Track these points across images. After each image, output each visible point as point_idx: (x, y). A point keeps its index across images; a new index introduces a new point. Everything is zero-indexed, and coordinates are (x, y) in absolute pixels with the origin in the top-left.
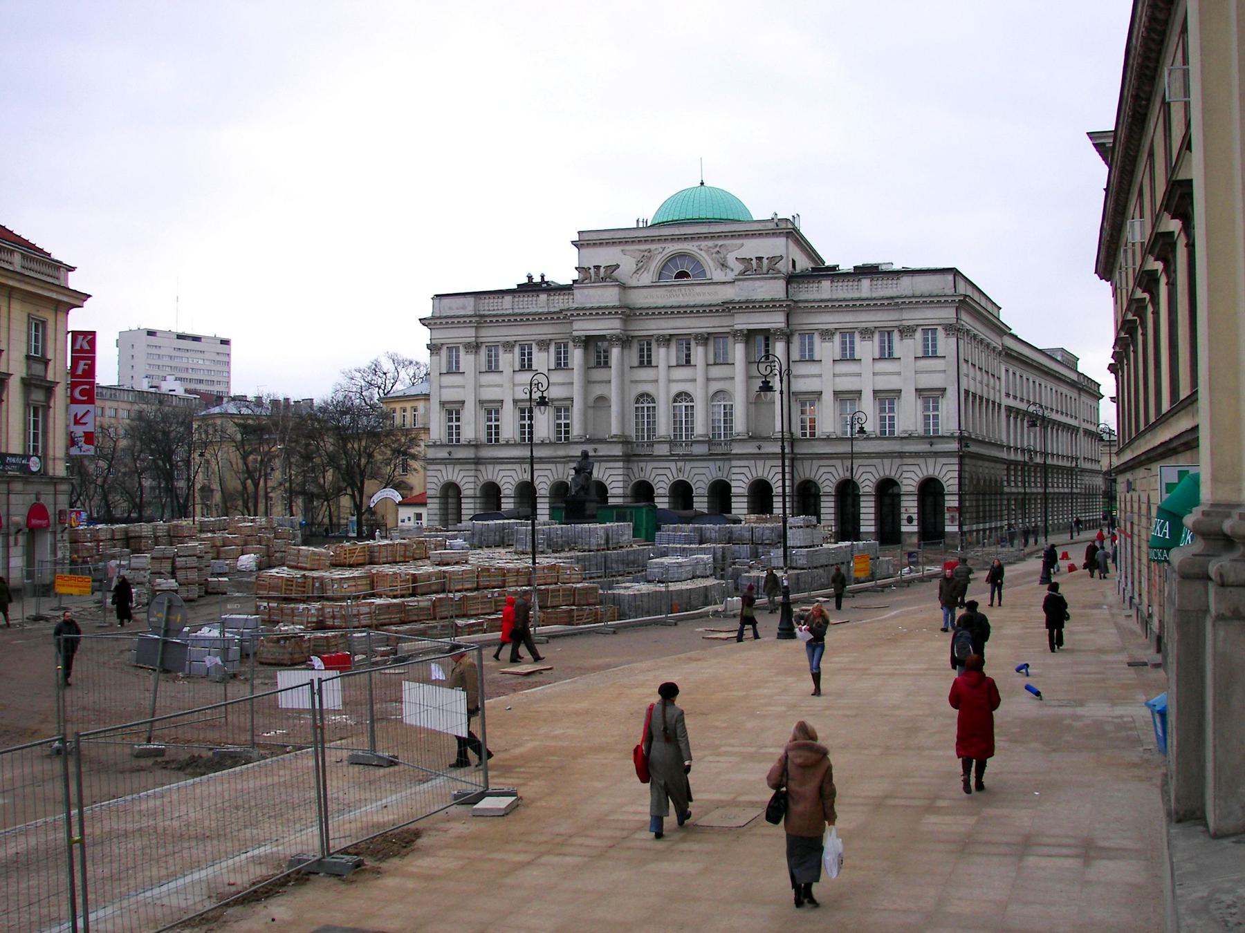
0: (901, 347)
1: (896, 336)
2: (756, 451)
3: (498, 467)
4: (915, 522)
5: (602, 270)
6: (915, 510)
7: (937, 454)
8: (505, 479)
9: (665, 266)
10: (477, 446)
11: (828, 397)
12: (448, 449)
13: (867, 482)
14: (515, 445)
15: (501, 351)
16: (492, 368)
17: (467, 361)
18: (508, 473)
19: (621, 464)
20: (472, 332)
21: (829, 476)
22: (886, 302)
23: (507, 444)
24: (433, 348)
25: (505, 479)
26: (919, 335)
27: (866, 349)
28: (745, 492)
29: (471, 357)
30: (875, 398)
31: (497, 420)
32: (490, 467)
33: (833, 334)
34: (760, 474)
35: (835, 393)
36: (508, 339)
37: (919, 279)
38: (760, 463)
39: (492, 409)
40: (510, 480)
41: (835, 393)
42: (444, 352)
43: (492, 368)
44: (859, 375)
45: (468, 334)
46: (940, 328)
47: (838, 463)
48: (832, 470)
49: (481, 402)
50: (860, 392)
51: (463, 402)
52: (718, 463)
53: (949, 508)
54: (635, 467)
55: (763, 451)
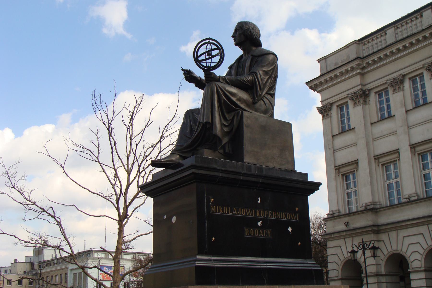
3: (403, 233)
8: (412, 248)
10: (373, 209)
12: (346, 219)
14: (419, 200)
15: (390, 91)
16: (386, 115)
17: (356, 113)
18: (414, 239)
20: (357, 80)
23: (410, 202)
24: (324, 111)
25: (412, 248)
29: (359, 109)
31: (396, 177)
32: (393, 234)
36: (395, 75)
39: (387, 161)
40: (417, 248)
42: (334, 112)
43: (386, 115)
45: (353, 83)
49: (377, 158)
51: (356, 162)
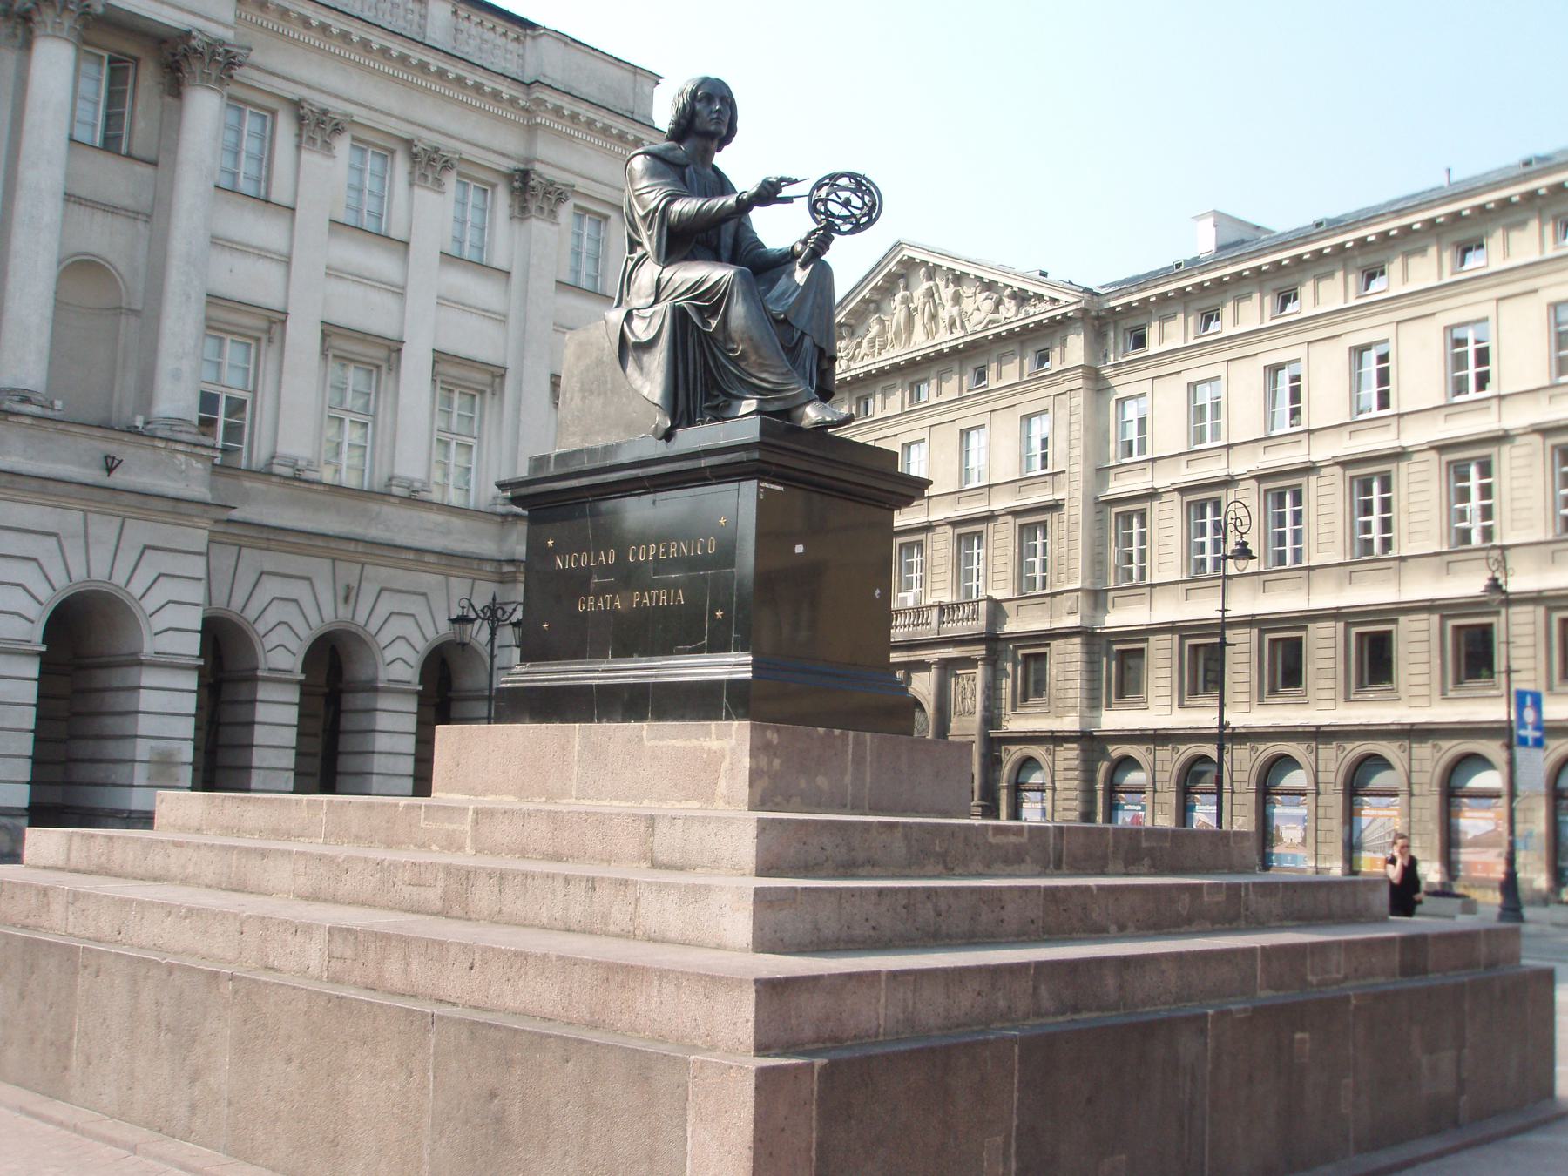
0: (505, 238)
1: (502, 199)
2: (95, 475)
11: (302, 336)
13: (401, 649)
21: (289, 613)
22: (507, 90)
26: (566, 212)
27: (431, 214)
28: (35, 635)
30: (434, 381)
33: (338, 129)
34: (100, 572)
35: (329, 331)
37: (578, 56)
38: (104, 528)
41: (329, 331)
44: (400, 292)
46: (614, 215)
47: (320, 568)
48: (299, 590)
50: (394, 348)
55: (119, 478)
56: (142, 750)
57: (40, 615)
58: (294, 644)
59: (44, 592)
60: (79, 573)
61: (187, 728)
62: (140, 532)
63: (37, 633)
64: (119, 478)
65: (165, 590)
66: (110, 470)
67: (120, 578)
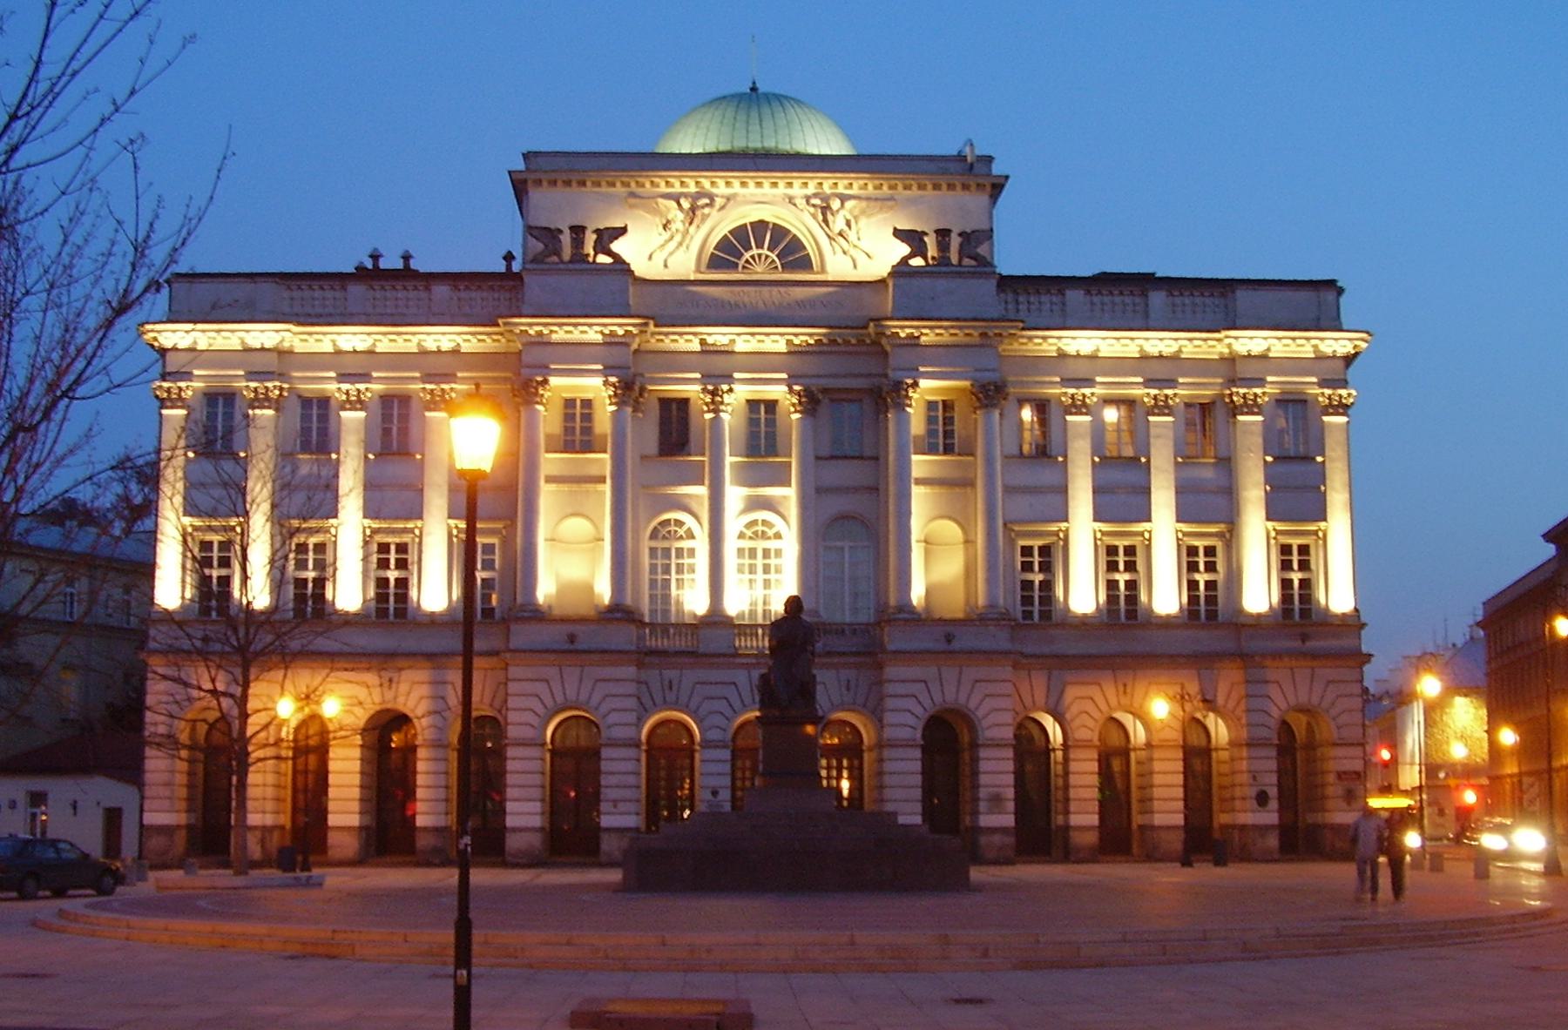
4: (1273, 804)
5: (590, 239)
6: (1274, 779)
7: (1315, 656)
9: (724, 244)
19: (630, 671)
21: (1089, 707)
34: (950, 697)
38: (950, 673)
52: (846, 674)
53: (1341, 775)
54: (652, 675)
55: (956, 645)
56: (983, 793)
57: (920, 725)
58: (1091, 723)
59: (918, 710)
60: (938, 698)
61: (1010, 779)
62: (971, 673)
63: (919, 734)
64: (956, 645)
65: (989, 704)
66: (949, 641)
67: (962, 700)
